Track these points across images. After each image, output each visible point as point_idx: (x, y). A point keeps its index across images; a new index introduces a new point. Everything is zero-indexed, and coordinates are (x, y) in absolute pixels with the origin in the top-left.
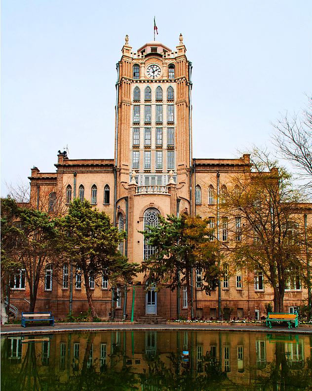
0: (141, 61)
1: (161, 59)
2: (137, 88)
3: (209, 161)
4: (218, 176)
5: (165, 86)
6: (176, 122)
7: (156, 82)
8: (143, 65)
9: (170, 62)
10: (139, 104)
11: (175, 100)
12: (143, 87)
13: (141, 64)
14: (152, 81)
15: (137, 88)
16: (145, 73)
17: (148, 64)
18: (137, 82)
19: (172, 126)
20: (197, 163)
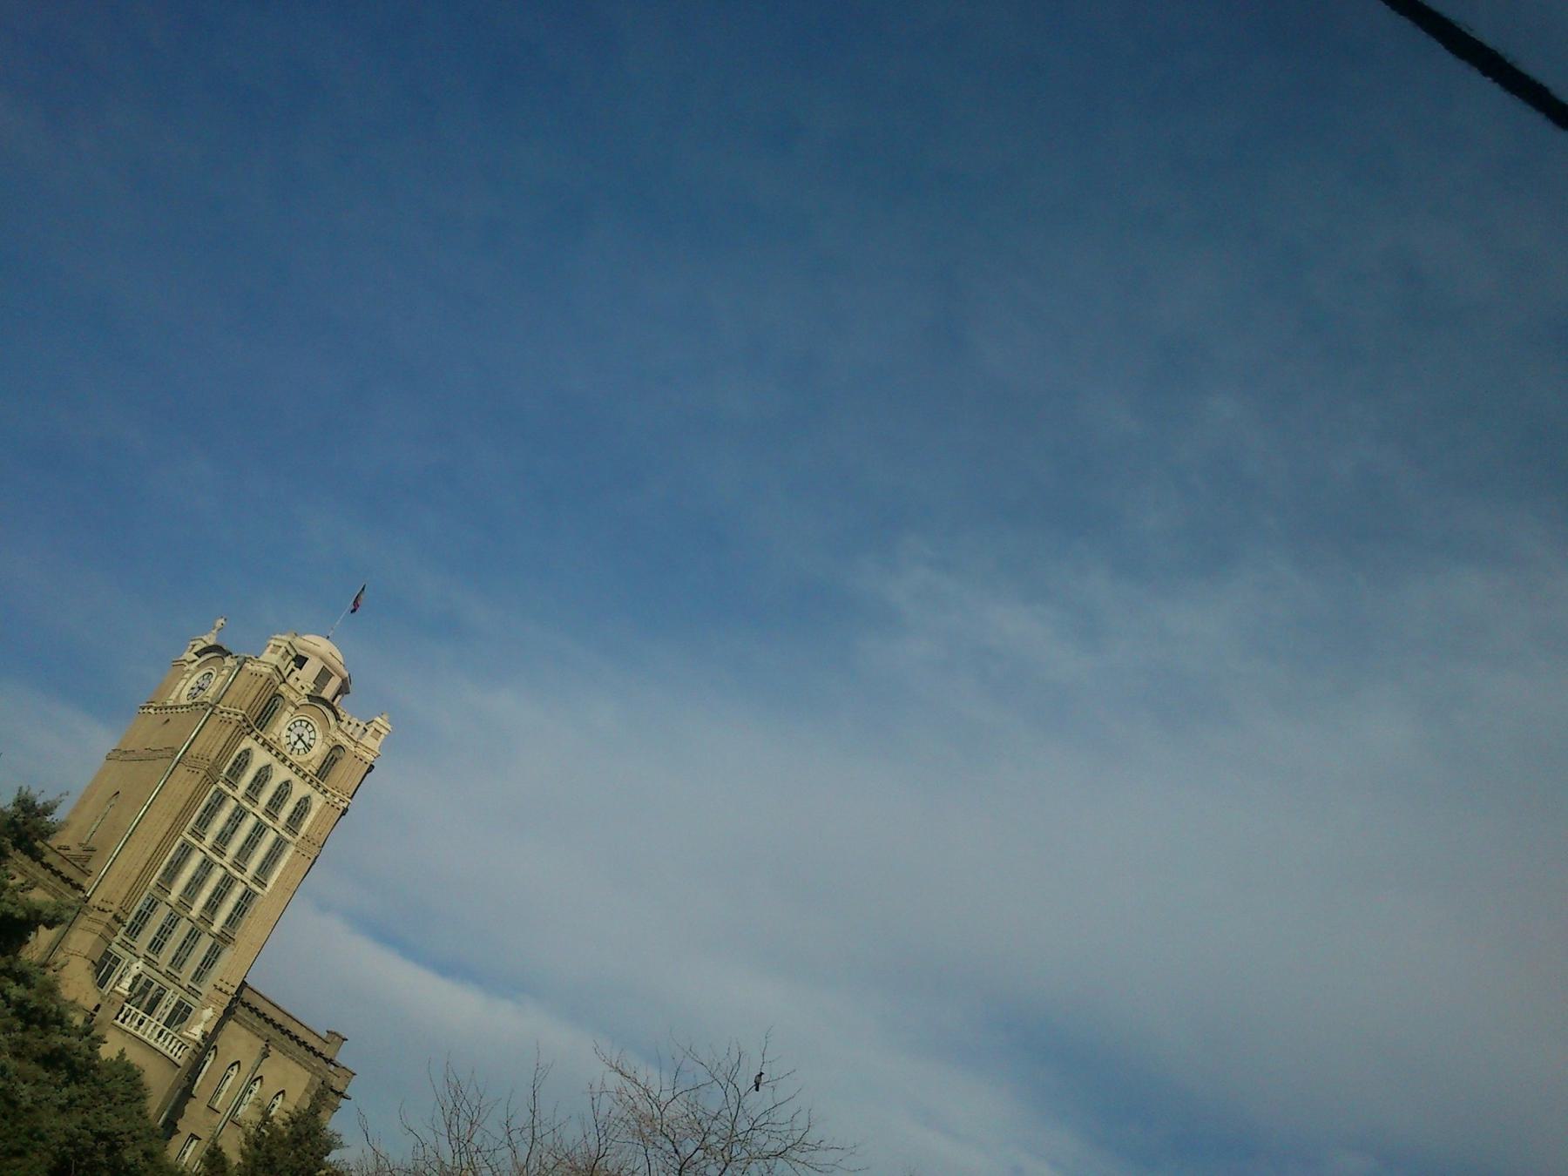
0: (292, 696)
1: (332, 721)
2: (247, 752)
3: (268, 1006)
4: (265, 1055)
5: (300, 789)
6: (270, 885)
7: (291, 766)
8: (292, 709)
9: (344, 741)
10: (230, 791)
11: (301, 835)
12: (261, 757)
13: (293, 704)
14: (284, 760)
15: (247, 752)
16: (282, 728)
17: (302, 715)
18: (256, 739)
19: (258, 890)
20: (246, 995)
